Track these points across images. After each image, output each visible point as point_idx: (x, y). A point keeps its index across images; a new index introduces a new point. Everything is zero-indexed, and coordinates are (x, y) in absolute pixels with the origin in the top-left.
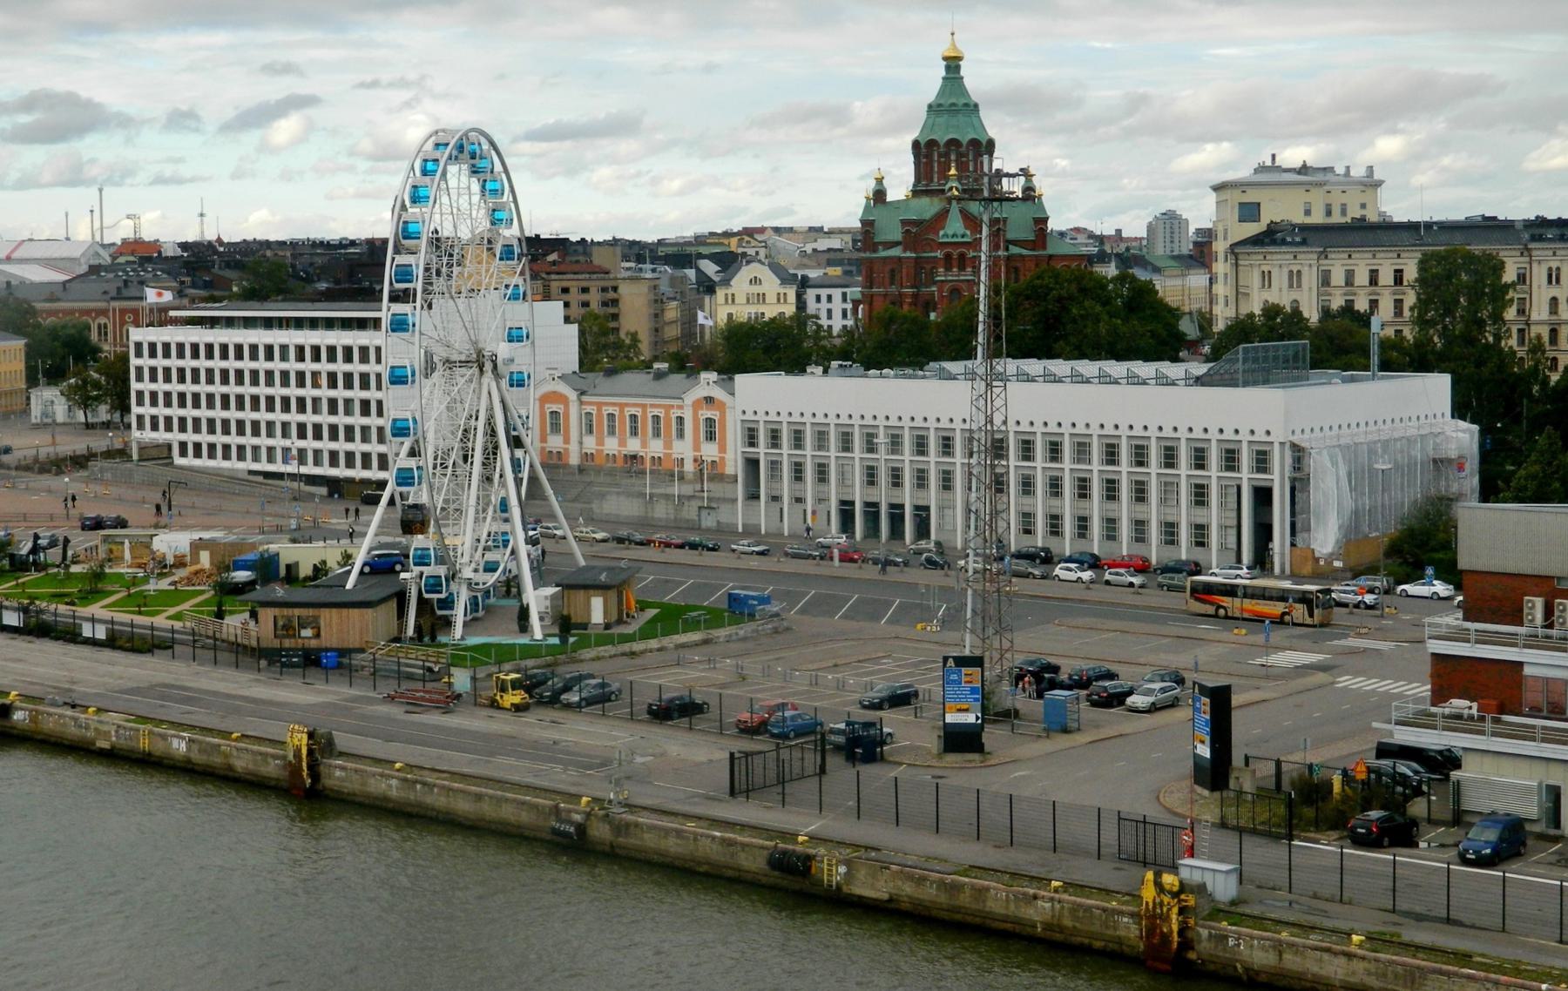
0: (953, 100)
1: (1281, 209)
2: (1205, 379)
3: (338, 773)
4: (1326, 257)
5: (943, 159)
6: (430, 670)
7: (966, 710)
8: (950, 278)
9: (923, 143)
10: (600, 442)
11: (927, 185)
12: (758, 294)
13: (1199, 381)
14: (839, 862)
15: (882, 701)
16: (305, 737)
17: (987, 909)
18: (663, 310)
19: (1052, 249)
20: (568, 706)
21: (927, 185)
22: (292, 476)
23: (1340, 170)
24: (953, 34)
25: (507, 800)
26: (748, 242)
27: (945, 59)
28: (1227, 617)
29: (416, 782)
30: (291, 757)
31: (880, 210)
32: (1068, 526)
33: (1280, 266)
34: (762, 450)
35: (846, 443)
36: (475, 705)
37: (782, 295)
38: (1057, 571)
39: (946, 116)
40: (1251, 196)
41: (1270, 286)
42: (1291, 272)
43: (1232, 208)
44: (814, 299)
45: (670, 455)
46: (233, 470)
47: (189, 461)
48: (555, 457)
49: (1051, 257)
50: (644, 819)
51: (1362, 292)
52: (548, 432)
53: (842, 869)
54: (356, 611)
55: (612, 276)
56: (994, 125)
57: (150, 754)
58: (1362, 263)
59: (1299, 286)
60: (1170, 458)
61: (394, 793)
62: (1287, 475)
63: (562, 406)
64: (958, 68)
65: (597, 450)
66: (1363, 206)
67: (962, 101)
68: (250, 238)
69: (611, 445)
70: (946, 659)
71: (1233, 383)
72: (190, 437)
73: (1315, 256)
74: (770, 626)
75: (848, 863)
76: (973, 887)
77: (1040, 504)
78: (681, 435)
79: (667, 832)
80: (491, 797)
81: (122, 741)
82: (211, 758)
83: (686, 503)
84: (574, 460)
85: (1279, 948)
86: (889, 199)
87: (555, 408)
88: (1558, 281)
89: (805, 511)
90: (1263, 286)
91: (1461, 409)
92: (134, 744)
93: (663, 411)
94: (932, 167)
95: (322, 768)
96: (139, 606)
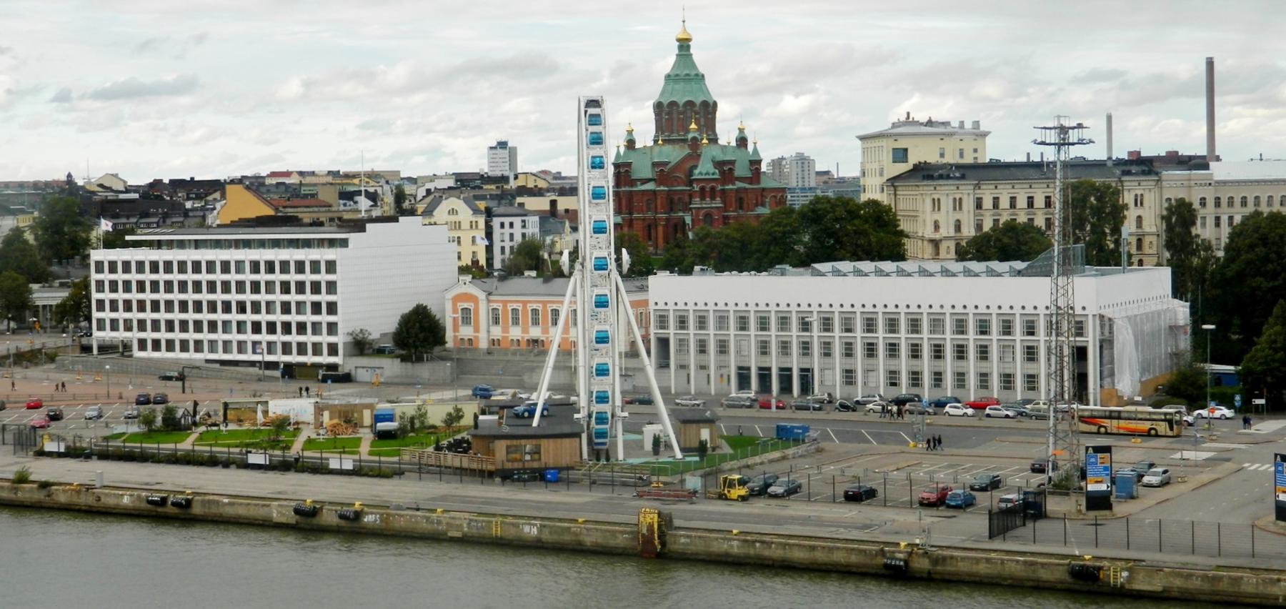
0: (687, 72)
1: (922, 153)
2: (1025, 272)
3: (683, 540)
4: (979, 188)
5: (682, 116)
6: (641, 478)
8: (704, 206)
10: (505, 330)
11: (669, 136)
12: (455, 222)
13: (1020, 273)
14: (1122, 569)
15: (987, 487)
16: (656, 516)
17: (1241, 590)
20: (776, 496)
21: (669, 136)
22: (252, 364)
23: (955, 124)
24: (684, 22)
25: (838, 548)
26: (368, 183)
27: (679, 40)
28: (1107, 433)
29: (756, 541)
30: (645, 531)
31: (632, 154)
32: (927, 379)
34: (672, 332)
35: (743, 324)
36: (706, 498)
38: (947, 409)
39: (682, 84)
40: (901, 144)
41: (939, 209)
42: (955, 199)
43: (888, 152)
45: (568, 339)
46: (191, 359)
47: (149, 354)
48: (466, 343)
49: (763, 189)
50: (956, 553)
51: (1040, 213)
52: (460, 323)
53: (1125, 574)
54: (551, 441)
55: (333, 209)
57: (501, 538)
58: (1005, 192)
60: (1007, 328)
61: (735, 550)
62: (1098, 338)
63: (473, 305)
64: (688, 47)
67: (693, 72)
69: (515, 333)
72: (149, 335)
74: (813, 447)
75: (1129, 569)
76: (1230, 577)
77: (904, 364)
78: (555, 323)
79: (978, 561)
80: (823, 548)
81: (474, 531)
82: (561, 537)
84: (483, 344)
86: (637, 146)
87: (466, 305)
88: (1142, 204)
90: (934, 210)
91: (1178, 292)
92: (486, 532)
95: (668, 537)
96: (344, 448)
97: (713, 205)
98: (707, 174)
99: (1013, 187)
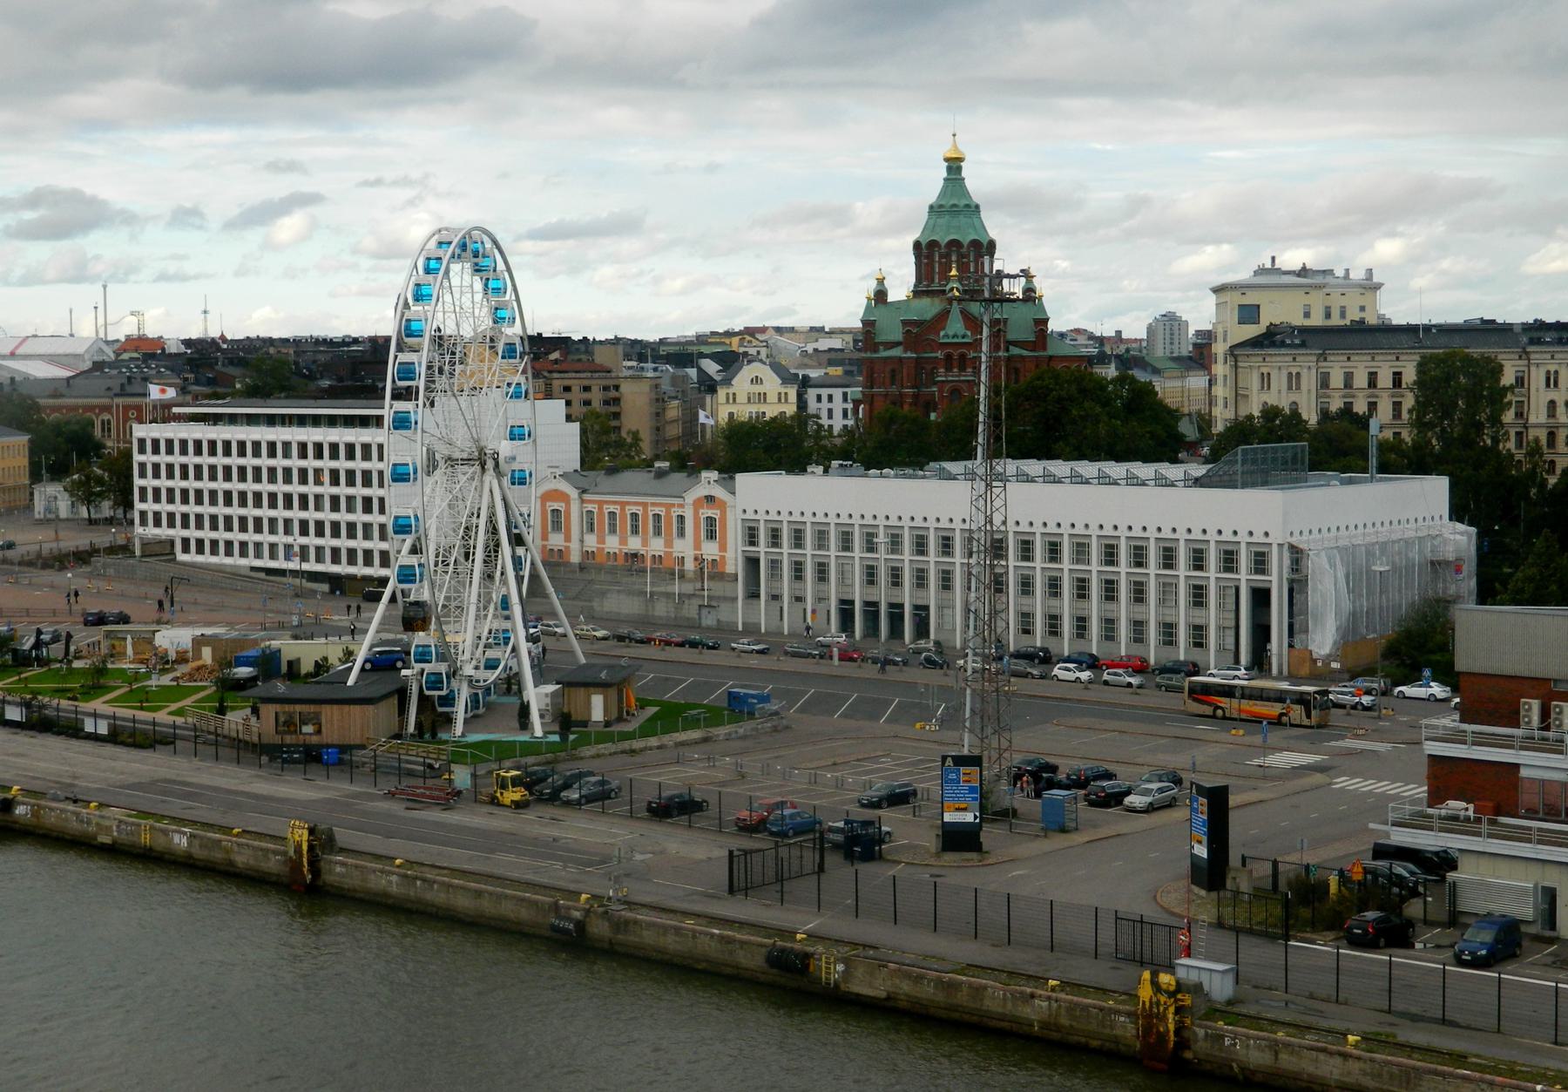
0: (956, 202)
1: (1280, 311)
3: (338, 869)
4: (1325, 360)
6: (431, 766)
7: (965, 809)
8: (950, 378)
9: (924, 244)
10: (601, 540)
11: (928, 286)
13: (1198, 482)
14: (837, 960)
15: (881, 799)
16: (306, 833)
17: (984, 1008)
18: (664, 409)
19: (1052, 350)
20: (568, 803)
21: (928, 286)
22: (295, 573)
23: (1339, 273)
24: (954, 135)
25: (506, 896)
26: (750, 342)
27: (947, 160)
28: (1224, 718)
29: (416, 878)
30: (291, 853)
31: (882, 308)
32: (1067, 627)
33: (1280, 368)
35: (846, 542)
36: (476, 801)
37: (783, 395)
38: (1056, 671)
39: (947, 217)
40: (1251, 299)
41: (1269, 388)
42: (1290, 374)
43: (1232, 309)
44: (815, 399)
46: (235, 566)
47: (192, 557)
49: (1051, 358)
51: (1360, 394)
53: (840, 967)
54: (358, 707)
55: (613, 375)
56: (994, 226)
57: (151, 849)
58: (1361, 366)
59: (1298, 388)
60: (1168, 559)
61: (394, 889)
62: (1285, 576)
63: (563, 505)
64: (959, 169)
65: (598, 548)
66: (1362, 309)
67: (963, 202)
68: (253, 335)
69: (612, 544)
70: (944, 758)
71: (1232, 485)
72: (193, 533)
73: (1315, 359)
74: (769, 725)
75: (846, 961)
76: (970, 985)
77: (1039, 604)
78: (681, 533)
79: (665, 929)
80: (491, 894)
81: (123, 836)
82: (212, 854)
83: (686, 602)
84: (575, 558)
85: (1275, 1047)
86: (890, 299)
87: (556, 506)
88: (1556, 384)
89: (805, 610)
90: (1263, 388)
91: (1457, 513)
92: (135, 839)
93: (664, 509)
94: (933, 268)
95: (322, 864)
96: (141, 702)
97: (962, 378)
98: (955, 336)
99: (1398, 359)
